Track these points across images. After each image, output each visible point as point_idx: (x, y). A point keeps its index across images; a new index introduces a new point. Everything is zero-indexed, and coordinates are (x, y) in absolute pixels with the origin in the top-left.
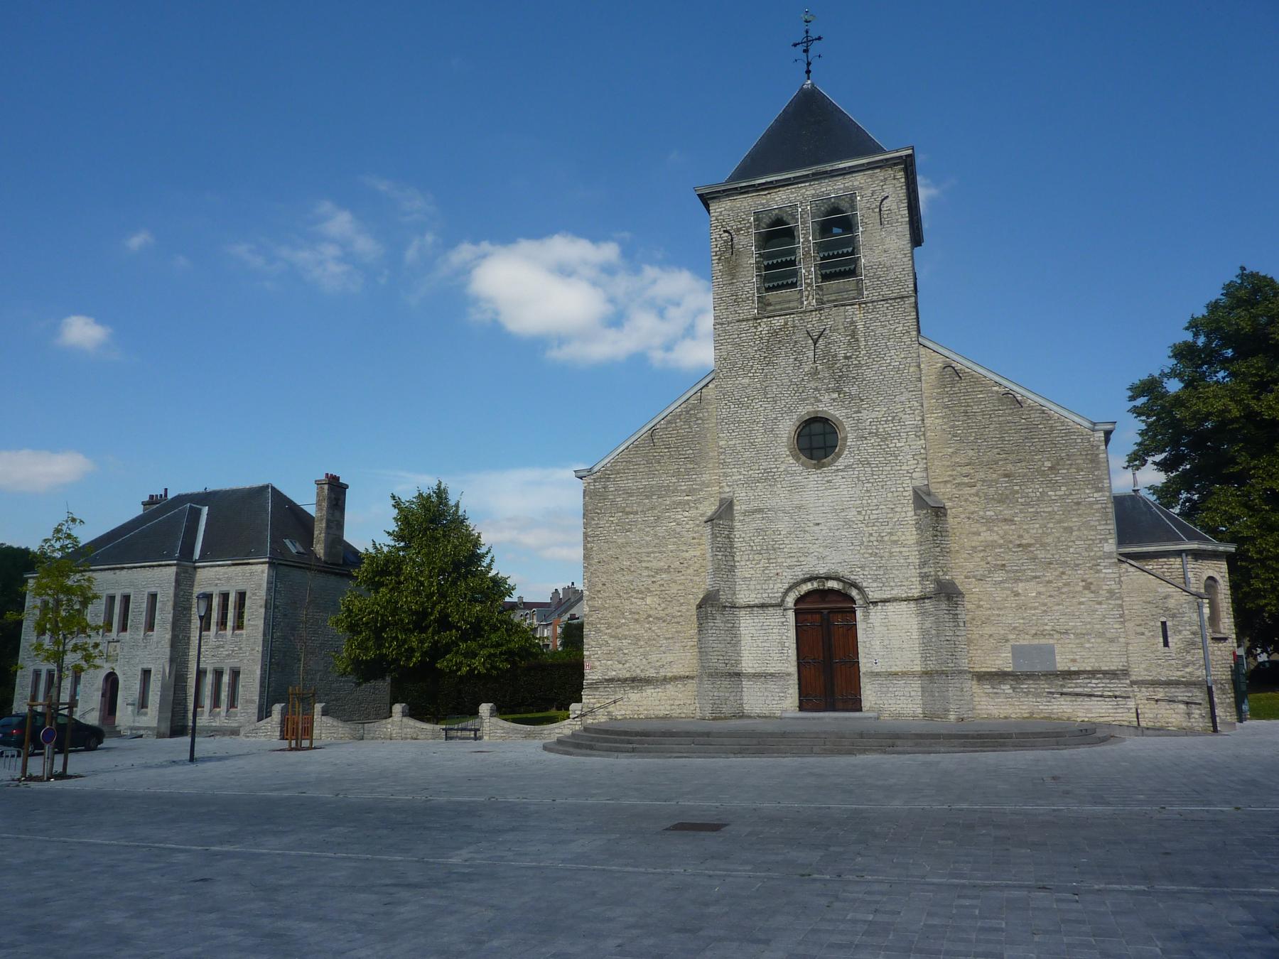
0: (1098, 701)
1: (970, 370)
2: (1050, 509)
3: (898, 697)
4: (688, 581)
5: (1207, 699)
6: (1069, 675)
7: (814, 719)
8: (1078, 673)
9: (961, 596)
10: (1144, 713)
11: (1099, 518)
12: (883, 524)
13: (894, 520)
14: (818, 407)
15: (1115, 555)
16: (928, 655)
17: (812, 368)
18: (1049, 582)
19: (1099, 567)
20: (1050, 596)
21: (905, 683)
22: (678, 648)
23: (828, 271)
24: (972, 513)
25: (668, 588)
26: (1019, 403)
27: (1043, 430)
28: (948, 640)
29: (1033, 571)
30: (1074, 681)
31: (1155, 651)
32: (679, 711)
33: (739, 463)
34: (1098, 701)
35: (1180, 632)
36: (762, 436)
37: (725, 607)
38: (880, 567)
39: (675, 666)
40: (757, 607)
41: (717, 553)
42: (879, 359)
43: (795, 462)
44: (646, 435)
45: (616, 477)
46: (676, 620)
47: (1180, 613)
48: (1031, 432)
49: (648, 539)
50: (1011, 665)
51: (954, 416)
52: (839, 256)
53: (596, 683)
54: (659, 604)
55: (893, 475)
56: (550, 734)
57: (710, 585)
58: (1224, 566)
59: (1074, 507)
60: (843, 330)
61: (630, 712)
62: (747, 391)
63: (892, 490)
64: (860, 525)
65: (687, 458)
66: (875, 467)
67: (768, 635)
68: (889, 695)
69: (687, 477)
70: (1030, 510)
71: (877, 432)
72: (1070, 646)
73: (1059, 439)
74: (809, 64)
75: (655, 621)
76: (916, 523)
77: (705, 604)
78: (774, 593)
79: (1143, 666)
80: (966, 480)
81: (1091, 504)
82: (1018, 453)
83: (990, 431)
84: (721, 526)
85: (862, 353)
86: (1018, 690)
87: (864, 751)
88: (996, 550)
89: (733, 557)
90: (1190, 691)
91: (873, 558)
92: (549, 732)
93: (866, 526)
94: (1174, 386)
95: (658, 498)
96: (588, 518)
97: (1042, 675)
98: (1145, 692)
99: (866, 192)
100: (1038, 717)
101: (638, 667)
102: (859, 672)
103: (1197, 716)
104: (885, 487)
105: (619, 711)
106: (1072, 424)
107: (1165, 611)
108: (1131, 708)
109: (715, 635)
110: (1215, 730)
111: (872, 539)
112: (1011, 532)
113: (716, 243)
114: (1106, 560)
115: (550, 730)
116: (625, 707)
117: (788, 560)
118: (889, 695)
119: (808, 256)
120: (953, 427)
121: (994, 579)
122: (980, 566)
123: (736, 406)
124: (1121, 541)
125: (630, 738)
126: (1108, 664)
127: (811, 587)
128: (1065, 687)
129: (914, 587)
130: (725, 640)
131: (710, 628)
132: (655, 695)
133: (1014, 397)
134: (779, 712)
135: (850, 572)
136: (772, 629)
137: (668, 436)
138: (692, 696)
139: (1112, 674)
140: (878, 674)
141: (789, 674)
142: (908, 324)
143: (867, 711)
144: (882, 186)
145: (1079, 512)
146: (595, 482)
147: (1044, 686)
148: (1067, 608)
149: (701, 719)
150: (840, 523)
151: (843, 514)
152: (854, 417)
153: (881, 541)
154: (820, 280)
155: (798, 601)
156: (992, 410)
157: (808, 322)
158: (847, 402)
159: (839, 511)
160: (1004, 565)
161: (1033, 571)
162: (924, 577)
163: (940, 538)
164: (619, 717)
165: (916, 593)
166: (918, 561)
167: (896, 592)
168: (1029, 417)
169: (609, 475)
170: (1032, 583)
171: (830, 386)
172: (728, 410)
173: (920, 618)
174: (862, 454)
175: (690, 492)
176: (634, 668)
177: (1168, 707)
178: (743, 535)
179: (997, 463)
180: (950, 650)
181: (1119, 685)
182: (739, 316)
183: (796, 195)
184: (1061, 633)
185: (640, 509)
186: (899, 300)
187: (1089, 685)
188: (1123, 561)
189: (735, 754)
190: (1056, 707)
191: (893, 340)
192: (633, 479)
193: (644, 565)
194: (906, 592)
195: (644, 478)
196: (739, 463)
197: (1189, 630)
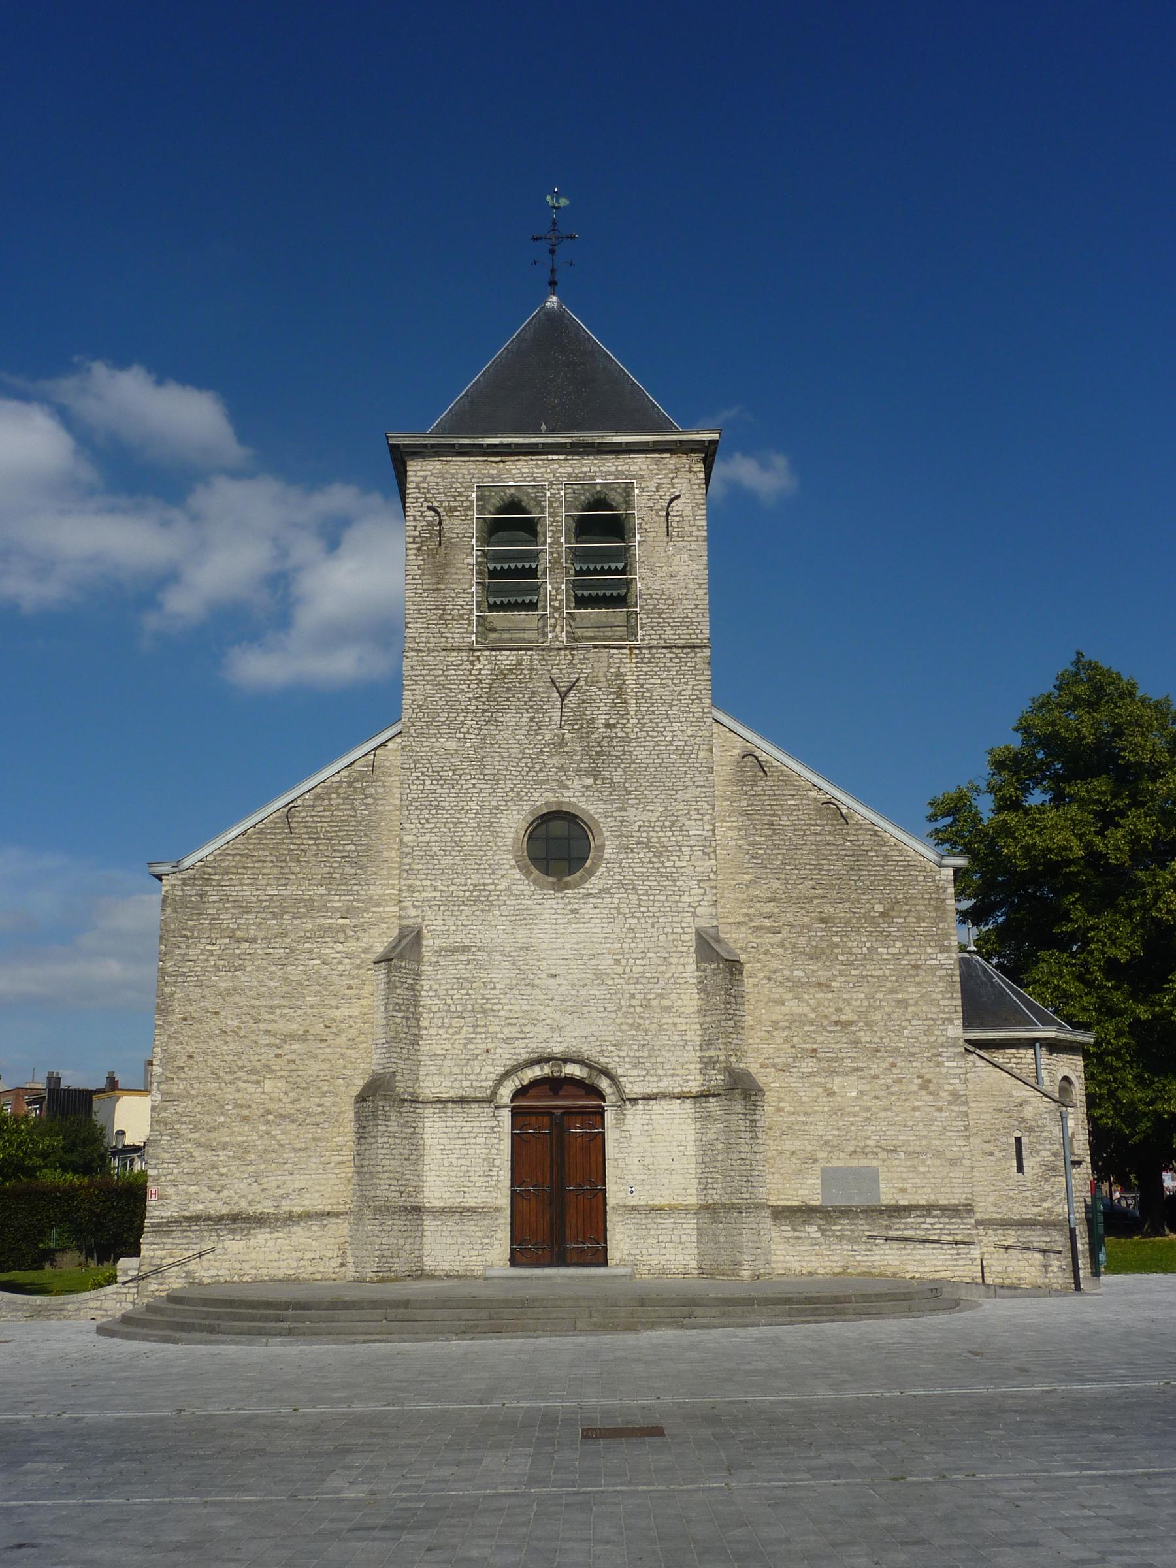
0: (933, 1249)
1: (779, 764)
2: (879, 973)
3: (663, 1245)
4: (337, 1057)
5: (1069, 1245)
6: (897, 1211)
7: (538, 1278)
8: (908, 1209)
9: (760, 1093)
10: (989, 1266)
11: (944, 989)
12: (651, 981)
13: (667, 976)
14: (563, 796)
15: (961, 1042)
16: (710, 1180)
17: (556, 735)
18: (875, 1077)
19: (940, 1059)
20: (876, 1097)
21: (674, 1223)
22: (314, 1166)
23: (586, 593)
24: (775, 972)
25: (301, 1067)
26: (844, 818)
27: (874, 859)
28: (743, 1159)
29: (854, 1059)
30: (903, 1221)
31: (1006, 1178)
32: (313, 1270)
33: (433, 872)
34: (933, 1249)
35: (1038, 1152)
36: (474, 833)
37: (405, 1100)
38: (644, 1045)
39: (308, 1195)
40: (454, 1102)
41: (395, 1014)
42: (655, 734)
43: (523, 877)
44: (278, 813)
45: (223, 880)
46: (313, 1119)
47: (1039, 1126)
48: (858, 861)
49: (272, 984)
50: (819, 1196)
51: (754, 828)
52: (603, 572)
53: (168, 1224)
54: (286, 1093)
55: (669, 909)
56: (79, 1309)
57: (379, 1064)
58: (1079, 1062)
59: (911, 972)
60: (606, 684)
61: (227, 1272)
62: (452, 760)
63: (666, 930)
64: (616, 981)
65: (346, 857)
66: (643, 895)
67: (468, 1146)
68: (649, 1241)
69: (343, 887)
70: (853, 972)
71: (649, 842)
72: (900, 1169)
73: (895, 873)
74: (553, 271)
75: (278, 1120)
76: (699, 982)
77: (374, 1095)
78: (481, 1081)
79: (991, 1199)
80: (767, 923)
81: (934, 969)
82: (840, 888)
83: (802, 854)
84: (403, 971)
85: (631, 721)
86: (828, 1233)
87: (652, 1325)
88: (806, 1028)
89: (418, 1020)
90: (1049, 1235)
91: (634, 1032)
92: (75, 1306)
93: (626, 983)
94: (985, 805)
95: (294, 918)
96: (170, 944)
97: (862, 1212)
98: (994, 1236)
99: (648, 484)
100: (853, 1271)
101: (243, 1196)
102: (605, 1204)
103: (1056, 1270)
104: (656, 925)
105: (207, 1271)
106: (912, 853)
107: (1020, 1123)
108: (975, 1259)
109: (388, 1146)
110: (1077, 1287)
111: (634, 1003)
112: (826, 1003)
113: (414, 523)
114: (950, 1049)
115: (79, 1302)
116: (217, 1264)
117: (506, 1030)
118: (649, 1241)
119: (557, 565)
120: (752, 844)
121: (801, 1070)
122: (782, 1049)
123: (434, 782)
124: (968, 1024)
125: (279, 1312)
126: (948, 1196)
127: (540, 1073)
128: (891, 1229)
129: (693, 1077)
130: (401, 1154)
131: (379, 1134)
132: (271, 1243)
133: (838, 808)
134: (481, 1268)
135: (599, 1052)
136: (475, 1138)
137: (315, 819)
138: (334, 1244)
139: (953, 1210)
140: (634, 1209)
141: (498, 1209)
142: (699, 687)
143: (617, 1265)
144: (673, 478)
145: (917, 979)
146: (185, 884)
147: (864, 1227)
148: (897, 1115)
149: (355, 1281)
150: (588, 976)
151: (593, 962)
152: (616, 817)
153: (647, 1006)
154: (573, 605)
155: (518, 1094)
156: (807, 825)
157: (553, 665)
158: (606, 794)
159: (588, 957)
160: (815, 1050)
161: (854, 1059)
162: (708, 1063)
163: (734, 1007)
164: (206, 1281)
165: (694, 1087)
166: (699, 1039)
167: (666, 1085)
168: (856, 838)
169: (210, 874)
170: (852, 1078)
171: (582, 765)
172: (421, 787)
173: (699, 1125)
174: (626, 874)
175: (347, 912)
176: (236, 1198)
177: (1020, 1257)
178: (436, 987)
179: (810, 901)
180: (745, 1173)
181: (962, 1227)
182: (446, 642)
183: (543, 470)
184: (888, 1151)
185: (260, 935)
186: (688, 650)
187: (923, 1226)
188: (970, 1052)
189: (456, 1334)
190: (878, 1258)
191: (677, 708)
192: (252, 885)
193: (263, 1026)
194: (681, 1086)
195: (271, 885)
196: (433, 872)
197: (1050, 1150)
